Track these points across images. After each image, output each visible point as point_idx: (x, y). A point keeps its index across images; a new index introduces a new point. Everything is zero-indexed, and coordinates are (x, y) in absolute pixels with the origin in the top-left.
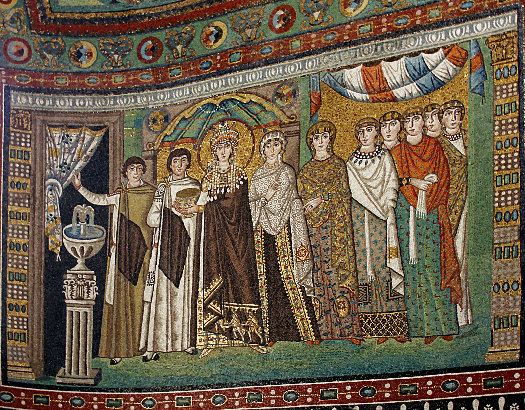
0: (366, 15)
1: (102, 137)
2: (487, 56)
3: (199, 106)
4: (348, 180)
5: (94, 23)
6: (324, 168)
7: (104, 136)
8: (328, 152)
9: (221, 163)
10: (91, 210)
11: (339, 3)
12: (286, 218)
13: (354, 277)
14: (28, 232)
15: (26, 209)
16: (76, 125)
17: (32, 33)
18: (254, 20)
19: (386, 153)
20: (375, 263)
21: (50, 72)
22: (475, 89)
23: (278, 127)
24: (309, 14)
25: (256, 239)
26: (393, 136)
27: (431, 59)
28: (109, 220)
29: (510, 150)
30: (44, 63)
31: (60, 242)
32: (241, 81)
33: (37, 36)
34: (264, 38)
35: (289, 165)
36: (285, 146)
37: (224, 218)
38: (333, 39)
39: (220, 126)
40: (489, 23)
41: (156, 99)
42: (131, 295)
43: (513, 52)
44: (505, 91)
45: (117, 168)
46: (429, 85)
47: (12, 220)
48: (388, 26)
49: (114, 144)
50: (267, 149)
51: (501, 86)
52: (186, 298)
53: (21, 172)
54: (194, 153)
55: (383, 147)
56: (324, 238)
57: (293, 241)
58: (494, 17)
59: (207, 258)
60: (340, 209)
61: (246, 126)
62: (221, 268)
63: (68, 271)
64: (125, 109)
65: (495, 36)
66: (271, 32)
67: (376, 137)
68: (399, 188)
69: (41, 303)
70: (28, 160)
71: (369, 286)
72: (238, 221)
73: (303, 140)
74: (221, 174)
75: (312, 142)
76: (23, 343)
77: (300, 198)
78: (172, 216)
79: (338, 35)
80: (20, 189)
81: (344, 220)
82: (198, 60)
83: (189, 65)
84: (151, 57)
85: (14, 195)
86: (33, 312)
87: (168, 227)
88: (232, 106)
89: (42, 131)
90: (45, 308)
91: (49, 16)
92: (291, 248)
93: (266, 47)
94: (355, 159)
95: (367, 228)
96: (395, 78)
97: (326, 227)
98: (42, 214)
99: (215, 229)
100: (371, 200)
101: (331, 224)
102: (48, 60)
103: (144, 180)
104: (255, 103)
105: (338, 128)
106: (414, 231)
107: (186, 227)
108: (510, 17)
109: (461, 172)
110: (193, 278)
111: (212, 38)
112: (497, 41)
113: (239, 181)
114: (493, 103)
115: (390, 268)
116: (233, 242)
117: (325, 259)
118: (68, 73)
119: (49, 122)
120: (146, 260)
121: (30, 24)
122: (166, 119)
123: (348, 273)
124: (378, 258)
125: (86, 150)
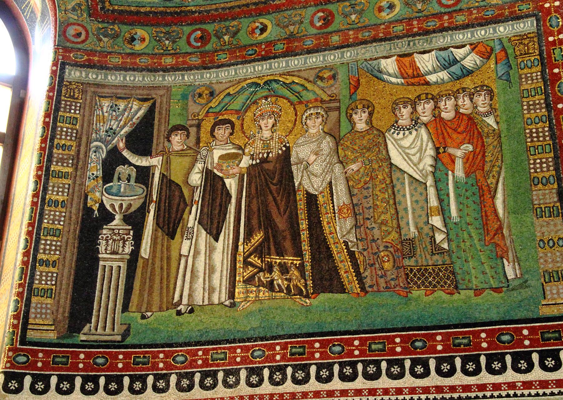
0: (399, 18)
1: (148, 107)
3: (244, 84)
4: (387, 148)
6: (364, 138)
7: (151, 106)
8: (367, 124)
9: (264, 132)
12: (328, 180)
13: (397, 232)
14: (69, 189)
15: (69, 168)
16: (124, 96)
18: (296, 19)
19: (422, 126)
20: (417, 221)
22: (502, 76)
23: (319, 103)
24: (346, 16)
25: (298, 198)
26: (428, 113)
27: (459, 53)
28: (150, 180)
29: (540, 125)
32: (284, 65)
33: (95, 22)
34: (306, 33)
36: (326, 119)
37: (266, 179)
38: (369, 36)
39: (264, 101)
40: (510, 27)
41: (202, 77)
43: (534, 48)
44: (530, 79)
46: (459, 73)
47: (54, 179)
48: (419, 27)
49: (160, 113)
50: (308, 121)
51: (526, 75)
52: (226, 251)
54: (237, 124)
55: (419, 121)
56: (366, 197)
57: (335, 200)
58: (514, 22)
59: (249, 214)
60: (381, 173)
61: (289, 101)
62: (262, 224)
63: (105, 227)
64: (172, 85)
65: (517, 36)
66: (312, 29)
67: (412, 113)
69: (73, 258)
70: (76, 125)
71: (412, 241)
72: (280, 182)
73: (343, 114)
74: (263, 141)
75: (352, 116)
76: (49, 299)
77: (341, 162)
78: (214, 176)
79: (373, 33)
81: (385, 182)
83: (235, 52)
84: (199, 44)
86: (64, 267)
87: (209, 186)
88: (275, 85)
90: (77, 263)
91: (107, 7)
92: (333, 206)
93: (308, 40)
94: (393, 130)
95: (407, 189)
96: (427, 67)
97: (368, 188)
98: (84, 173)
100: (410, 166)
101: (373, 186)
103: (188, 145)
104: (297, 83)
105: (376, 105)
106: (454, 192)
107: (228, 186)
108: (529, 22)
109: (495, 143)
110: (233, 232)
111: (258, 32)
112: (518, 40)
114: (520, 87)
115: (432, 225)
116: (275, 199)
117: (367, 216)
118: (121, 54)
120: (185, 216)
121: (90, 13)
122: (212, 94)
124: (420, 216)
125: (133, 118)
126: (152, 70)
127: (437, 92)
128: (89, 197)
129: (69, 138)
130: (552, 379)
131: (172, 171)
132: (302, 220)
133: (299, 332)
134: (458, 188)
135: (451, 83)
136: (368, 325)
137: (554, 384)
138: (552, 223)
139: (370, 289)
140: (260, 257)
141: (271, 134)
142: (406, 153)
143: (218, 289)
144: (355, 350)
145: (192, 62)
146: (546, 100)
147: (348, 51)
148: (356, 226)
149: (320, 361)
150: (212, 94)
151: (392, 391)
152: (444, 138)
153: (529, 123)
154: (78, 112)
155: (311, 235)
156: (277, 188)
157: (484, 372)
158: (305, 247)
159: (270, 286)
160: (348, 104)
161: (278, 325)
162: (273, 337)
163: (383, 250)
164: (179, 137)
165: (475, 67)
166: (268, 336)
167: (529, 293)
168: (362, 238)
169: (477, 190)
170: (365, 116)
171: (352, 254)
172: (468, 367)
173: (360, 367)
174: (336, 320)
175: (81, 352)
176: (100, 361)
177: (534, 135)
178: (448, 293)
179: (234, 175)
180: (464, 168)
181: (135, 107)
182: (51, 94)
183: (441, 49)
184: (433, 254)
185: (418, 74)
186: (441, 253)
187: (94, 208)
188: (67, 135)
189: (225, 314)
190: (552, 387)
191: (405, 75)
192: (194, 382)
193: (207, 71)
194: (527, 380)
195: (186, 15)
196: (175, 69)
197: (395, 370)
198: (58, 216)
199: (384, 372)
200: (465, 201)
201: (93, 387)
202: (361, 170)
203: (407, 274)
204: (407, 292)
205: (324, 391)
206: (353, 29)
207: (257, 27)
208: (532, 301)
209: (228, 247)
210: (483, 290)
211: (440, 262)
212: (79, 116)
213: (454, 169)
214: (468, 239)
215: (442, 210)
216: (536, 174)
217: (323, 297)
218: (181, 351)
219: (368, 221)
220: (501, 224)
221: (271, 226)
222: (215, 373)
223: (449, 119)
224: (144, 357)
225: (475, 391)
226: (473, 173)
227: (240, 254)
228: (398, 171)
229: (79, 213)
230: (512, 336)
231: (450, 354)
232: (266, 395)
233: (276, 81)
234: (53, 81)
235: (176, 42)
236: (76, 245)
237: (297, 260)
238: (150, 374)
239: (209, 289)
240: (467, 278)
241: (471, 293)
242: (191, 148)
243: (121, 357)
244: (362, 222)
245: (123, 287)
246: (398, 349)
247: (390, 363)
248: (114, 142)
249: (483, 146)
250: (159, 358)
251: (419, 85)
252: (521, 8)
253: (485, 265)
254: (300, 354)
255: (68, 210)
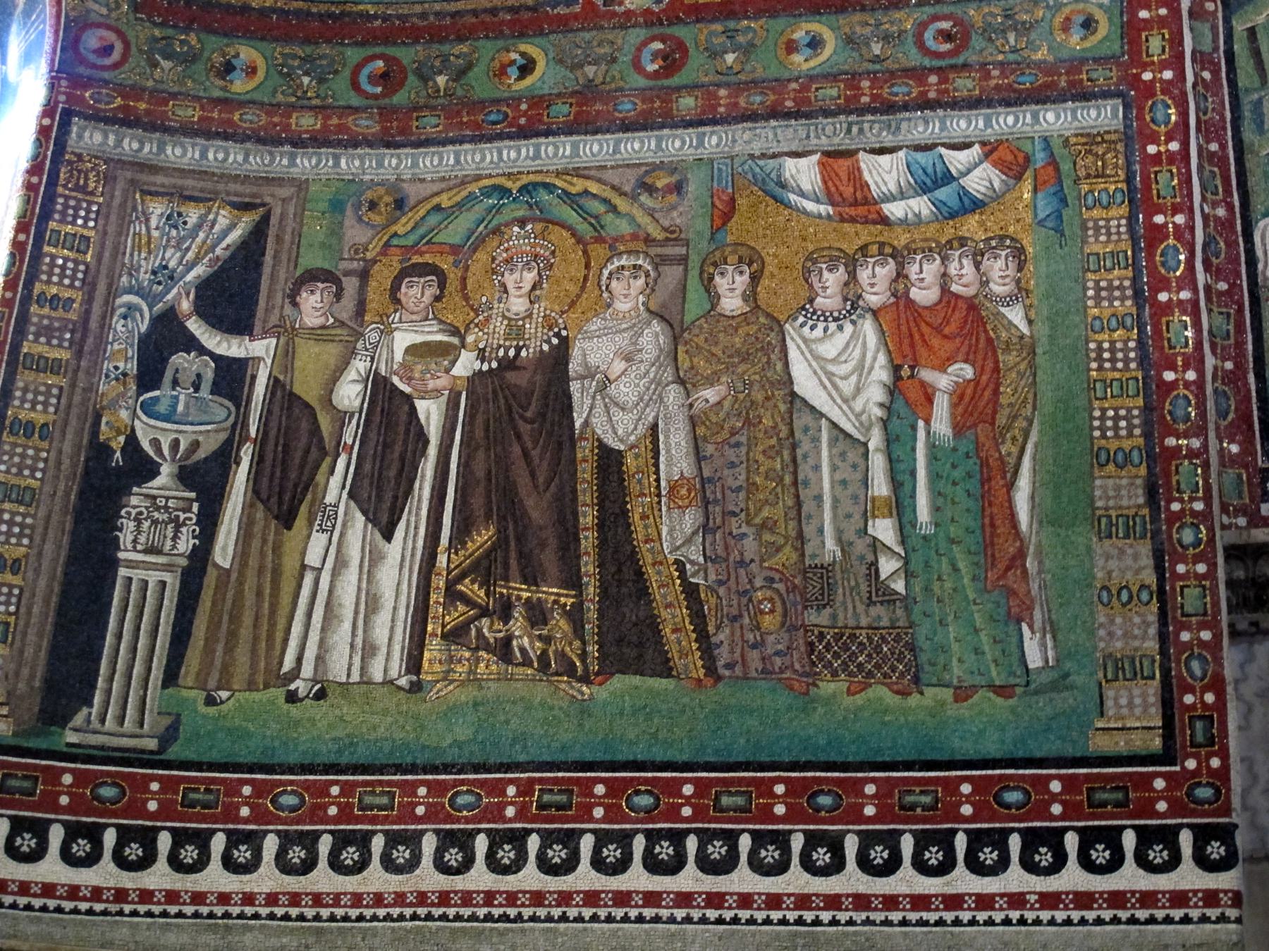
2: (1066, 167)
3: (474, 188)
4: (786, 356)
5: (268, 16)
6: (736, 330)
7: (259, 222)
8: (745, 298)
9: (512, 299)
10: (206, 365)
11: (776, 44)
12: (650, 419)
13: (796, 549)
14: (59, 398)
15: (62, 351)
17: (136, 19)
21: (163, 92)
22: (1045, 219)
24: (715, 54)
25: (579, 456)
27: (957, 160)
30: (152, 75)
31: (126, 427)
32: (568, 153)
34: (622, 84)
35: (661, 317)
36: (655, 281)
38: (762, 103)
39: (516, 229)
40: (1069, 114)
41: (380, 164)
42: (277, 549)
45: (279, 287)
47: (27, 372)
49: (279, 239)
50: (614, 284)
51: (1096, 221)
52: (407, 564)
53: (66, 277)
54: (453, 276)
55: (861, 303)
56: (732, 465)
57: (662, 467)
58: (1077, 104)
60: (769, 413)
61: (573, 235)
63: (135, 489)
64: (311, 177)
65: (1082, 135)
66: (636, 76)
68: (894, 384)
69: (59, 555)
70: (85, 253)
71: (828, 571)
72: (543, 415)
73: (694, 274)
74: (510, 319)
77: (681, 381)
78: (391, 392)
79: (772, 97)
80: (55, 309)
82: (481, 105)
83: (459, 113)
84: (379, 90)
85: (40, 321)
88: (544, 196)
89: (125, 201)
92: (658, 480)
93: (626, 100)
94: (801, 319)
95: (825, 453)
97: (738, 445)
99: (488, 426)
100: (834, 401)
101: (749, 439)
102: (162, 69)
103: (336, 315)
104: (594, 196)
105: (768, 260)
107: (422, 417)
108: (1109, 108)
111: (513, 72)
112: (1084, 144)
113: (549, 339)
114: (1082, 248)
115: (875, 538)
116: (526, 454)
117: (731, 508)
118: (198, 99)
119: (145, 183)
120: (320, 478)
123: (782, 541)
124: (849, 516)
126: (267, 139)
127: (903, 242)
128: (104, 420)
129: (67, 281)
130: (1100, 889)
131: (296, 373)
132: (585, 505)
133: (562, 758)
134: (936, 459)
135: (936, 225)
136: (717, 751)
137: (1105, 900)
138: (1129, 551)
139: (727, 673)
140: (485, 583)
141: (528, 305)
142: (826, 372)
143: (384, 650)
144: (683, 805)
145: (358, 129)
146: (1135, 280)
147: (712, 133)
148: (706, 528)
149: (603, 826)
150: (400, 204)
151: (759, 901)
152: (912, 345)
153: (1097, 328)
154: (91, 224)
155: (603, 543)
156: (532, 430)
157: (961, 869)
158: (588, 566)
159: (504, 649)
160: (705, 252)
161: (514, 739)
162: (502, 765)
163: (761, 588)
164: (317, 297)
165: (990, 193)
166: (492, 761)
167: (1071, 701)
168: (717, 557)
169: (977, 468)
170: (742, 281)
171: (691, 591)
172: (927, 855)
173: (692, 844)
174: (647, 737)
175: (65, 770)
176: (108, 792)
177: (1106, 355)
178: (897, 692)
179: (437, 392)
180: (953, 416)
181: (223, 222)
182: (35, 180)
183: (919, 148)
184: (871, 603)
185: (865, 198)
186: (888, 602)
187: (113, 445)
188: (62, 276)
189: (397, 705)
190: (1100, 908)
191: (837, 198)
192: (317, 854)
193: (393, 151)
194: (1050, 889)
195: (355, 22)
196: (318, 141)
197: (770, 854)
198: (32, 458)
199: (744, 858)
200: (949, 490)
201: (88, 848)
202: (727, 404)
203: (811, 644)
204: (808, 685)
205: (609, 892)
206: (727, 85)
207: (513, 62)
208: (1074, 718)
209: (413, 555)
210: (974, 688)
211: (885, 622)
212: (92, 233)
213: (930, 415)
214: (949, 575)
215: (897, 507)
216: (1103, 442)
217: (619, 682)
218: (291, 783)
219: (734, 520)
220: (1022, 545)
221: (514, 515)
222: (365, 838)
223: (928, 304)
224: (208, 791)
225: (937, 909)
226: (969, 428)
227: (439, 574)
228: (807, 411)
229: (79, 455)
230: (1027, 793)
231: (892, 827)
232: (478, 892)
233: (548, 187)
234: (42, 150)
235: (326, 80)
236: (68, 527)
237: (567, 596)
238: (220, 830)
239: (363, 649)
240: (941, 660)
241: (947, 694)
242: (342, 324)
243: (155, 786)
244: (718, 521)
245: (170, 631)
246: (780, 810)
247: (760, 839)
248: (169, 297)
249: (996, 369)
250: (241, 795)
251: (866, 222)
252: (1094, 75)
253: (984, 637)
254: (560, 807)
255: (54, 445)
